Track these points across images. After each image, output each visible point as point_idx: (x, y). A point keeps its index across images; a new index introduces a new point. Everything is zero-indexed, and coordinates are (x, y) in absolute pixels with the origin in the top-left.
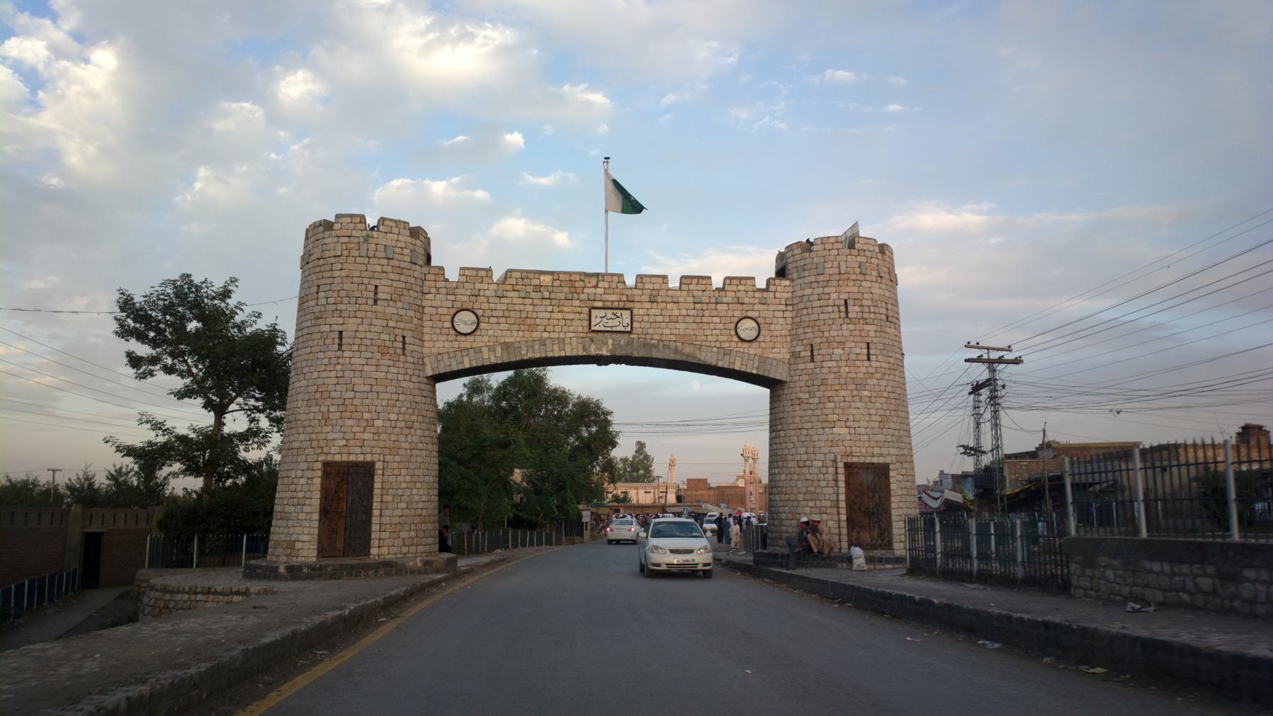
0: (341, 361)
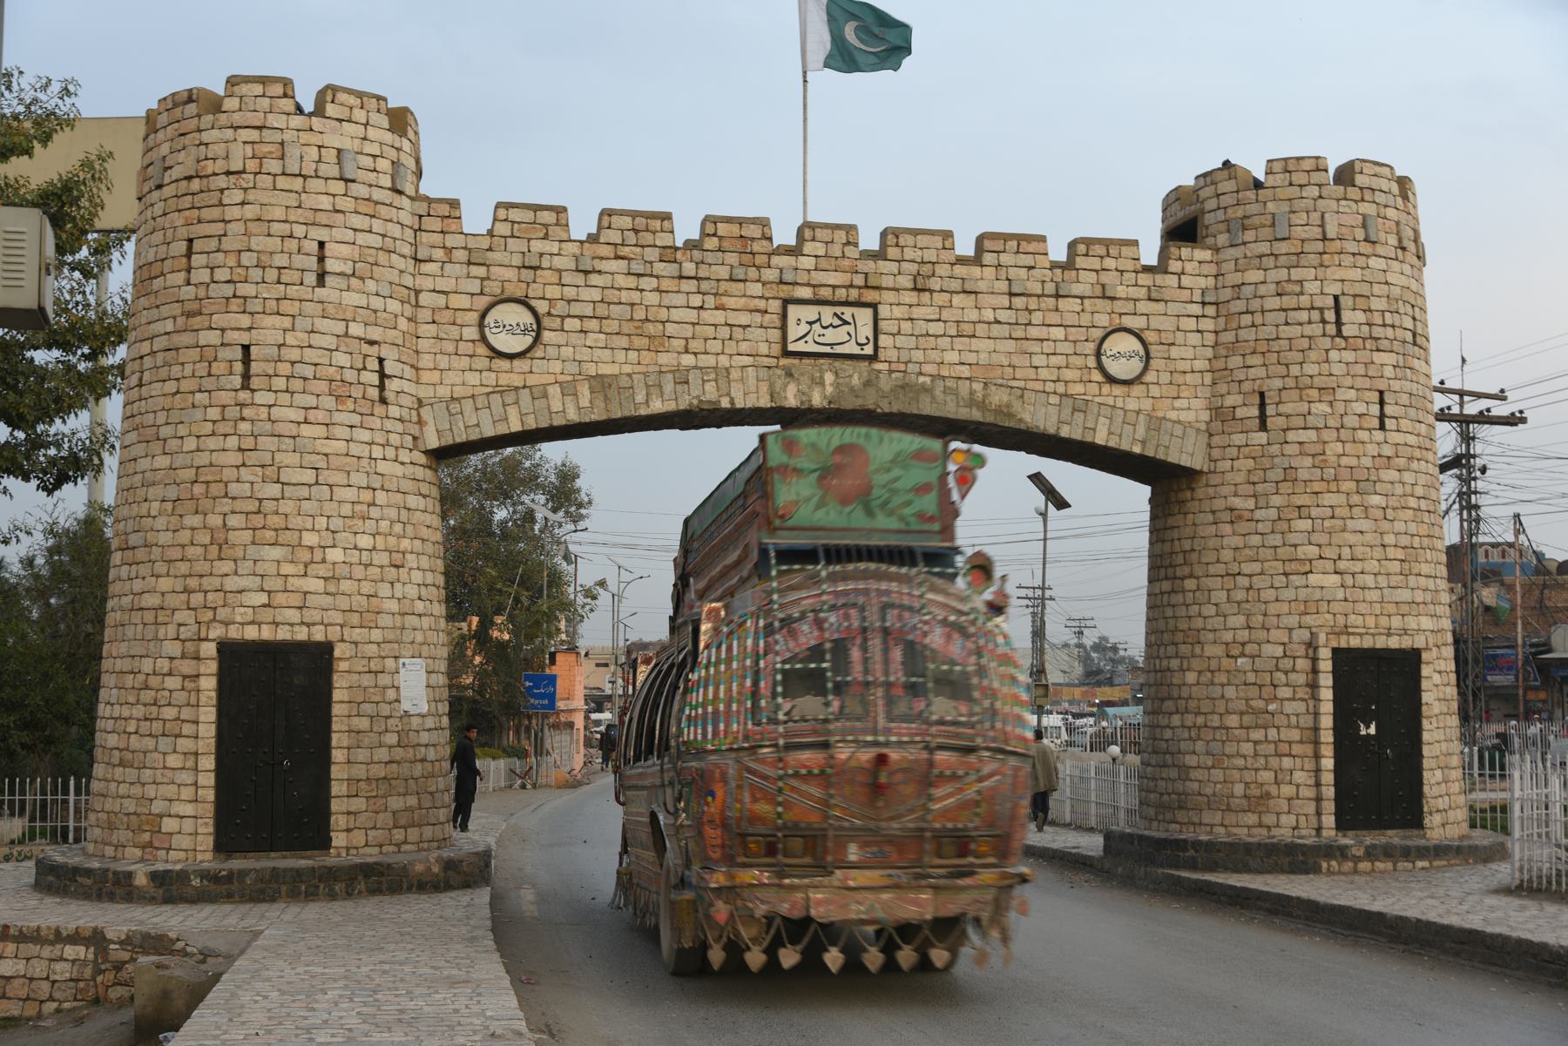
0: (247, 412)
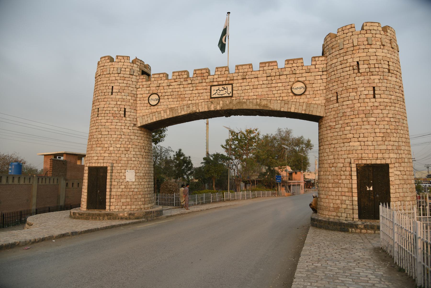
0: (98, 121)
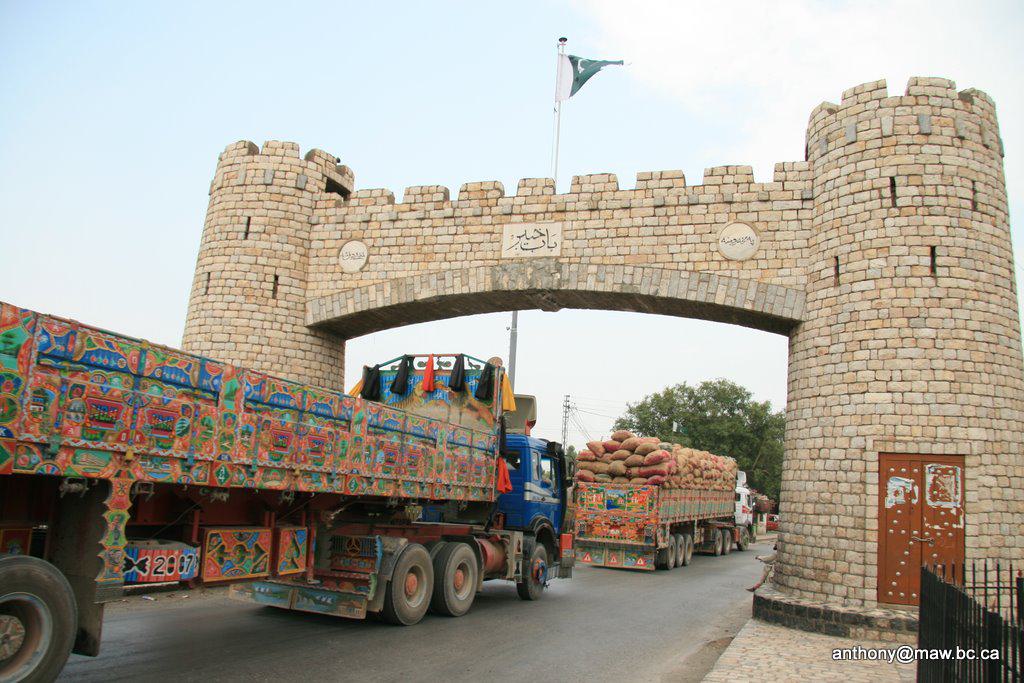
0: (205, 306)
